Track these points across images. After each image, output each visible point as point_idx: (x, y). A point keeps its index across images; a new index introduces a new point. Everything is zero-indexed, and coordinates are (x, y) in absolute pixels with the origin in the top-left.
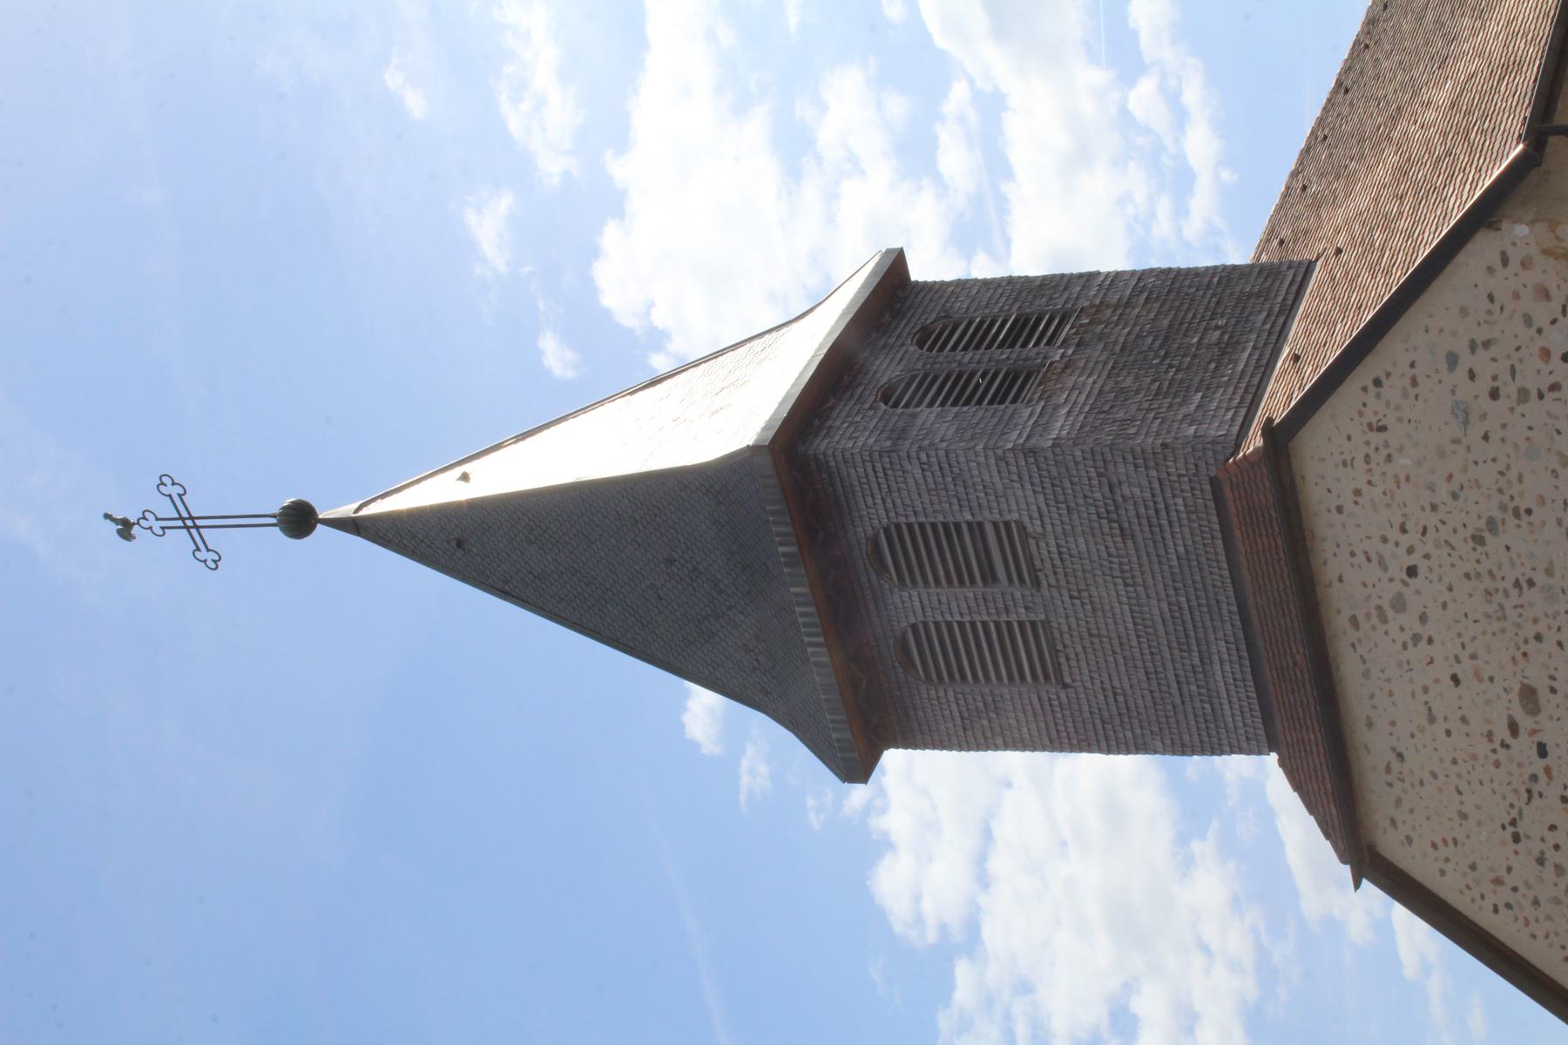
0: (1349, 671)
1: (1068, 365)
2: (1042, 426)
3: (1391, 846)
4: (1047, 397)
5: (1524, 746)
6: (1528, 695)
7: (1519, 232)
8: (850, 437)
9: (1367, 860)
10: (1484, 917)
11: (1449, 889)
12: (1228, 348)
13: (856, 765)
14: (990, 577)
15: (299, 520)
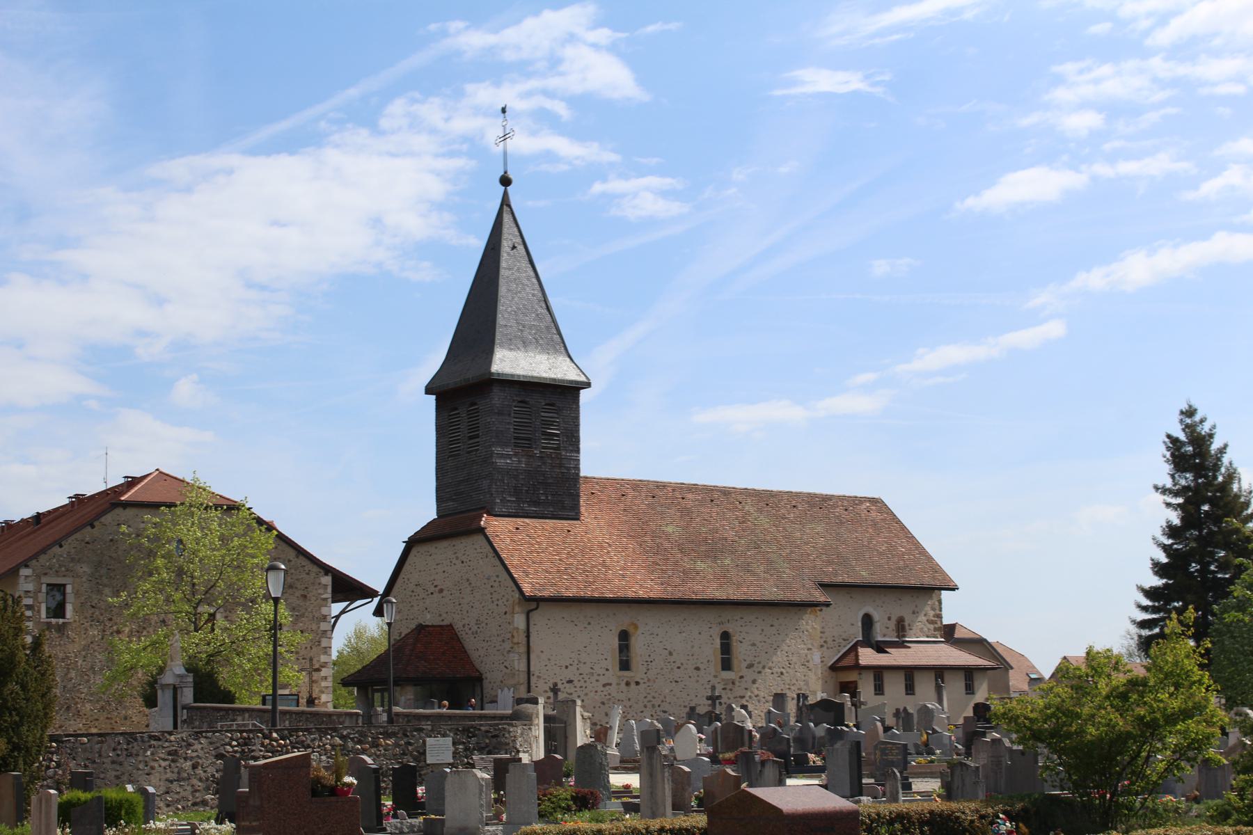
0: (443, 544)
1: (533, 456)
2: (502, 456)
3: (414, 552)
4: (516, 455)
5: (432, 589)
6: (441, 591)
7: (517, 595)
8: (498, 398)
9: (412, 543)
10: (402, 575)
11: (407, 567)
12: (536, 503)
13: (429, 390)
14: (471, 438)
15: (505, 181)
